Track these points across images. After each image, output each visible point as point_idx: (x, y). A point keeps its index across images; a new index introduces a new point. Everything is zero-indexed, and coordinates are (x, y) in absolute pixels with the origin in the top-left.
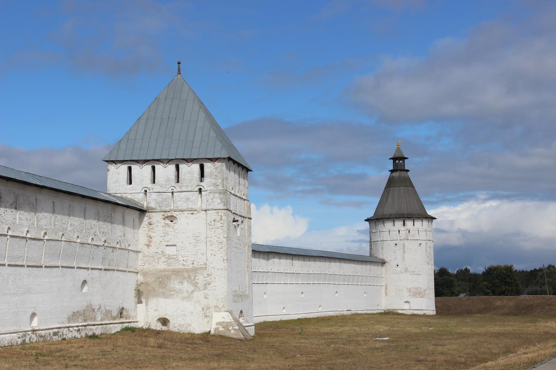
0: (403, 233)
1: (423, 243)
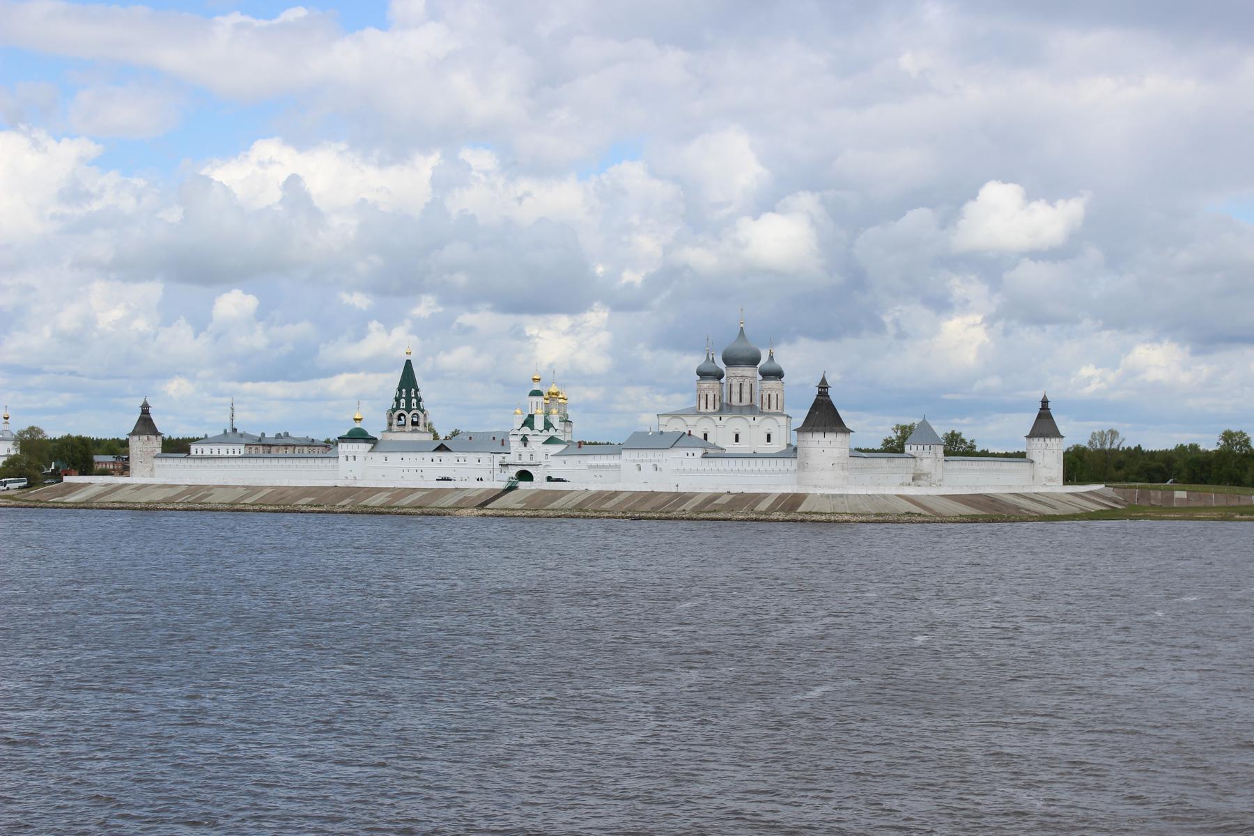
0: (1044, 445)
1: (1056, 452)
